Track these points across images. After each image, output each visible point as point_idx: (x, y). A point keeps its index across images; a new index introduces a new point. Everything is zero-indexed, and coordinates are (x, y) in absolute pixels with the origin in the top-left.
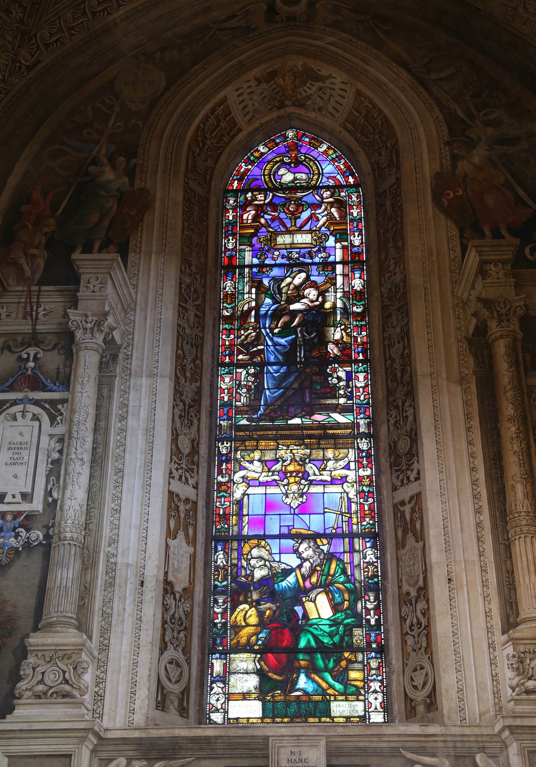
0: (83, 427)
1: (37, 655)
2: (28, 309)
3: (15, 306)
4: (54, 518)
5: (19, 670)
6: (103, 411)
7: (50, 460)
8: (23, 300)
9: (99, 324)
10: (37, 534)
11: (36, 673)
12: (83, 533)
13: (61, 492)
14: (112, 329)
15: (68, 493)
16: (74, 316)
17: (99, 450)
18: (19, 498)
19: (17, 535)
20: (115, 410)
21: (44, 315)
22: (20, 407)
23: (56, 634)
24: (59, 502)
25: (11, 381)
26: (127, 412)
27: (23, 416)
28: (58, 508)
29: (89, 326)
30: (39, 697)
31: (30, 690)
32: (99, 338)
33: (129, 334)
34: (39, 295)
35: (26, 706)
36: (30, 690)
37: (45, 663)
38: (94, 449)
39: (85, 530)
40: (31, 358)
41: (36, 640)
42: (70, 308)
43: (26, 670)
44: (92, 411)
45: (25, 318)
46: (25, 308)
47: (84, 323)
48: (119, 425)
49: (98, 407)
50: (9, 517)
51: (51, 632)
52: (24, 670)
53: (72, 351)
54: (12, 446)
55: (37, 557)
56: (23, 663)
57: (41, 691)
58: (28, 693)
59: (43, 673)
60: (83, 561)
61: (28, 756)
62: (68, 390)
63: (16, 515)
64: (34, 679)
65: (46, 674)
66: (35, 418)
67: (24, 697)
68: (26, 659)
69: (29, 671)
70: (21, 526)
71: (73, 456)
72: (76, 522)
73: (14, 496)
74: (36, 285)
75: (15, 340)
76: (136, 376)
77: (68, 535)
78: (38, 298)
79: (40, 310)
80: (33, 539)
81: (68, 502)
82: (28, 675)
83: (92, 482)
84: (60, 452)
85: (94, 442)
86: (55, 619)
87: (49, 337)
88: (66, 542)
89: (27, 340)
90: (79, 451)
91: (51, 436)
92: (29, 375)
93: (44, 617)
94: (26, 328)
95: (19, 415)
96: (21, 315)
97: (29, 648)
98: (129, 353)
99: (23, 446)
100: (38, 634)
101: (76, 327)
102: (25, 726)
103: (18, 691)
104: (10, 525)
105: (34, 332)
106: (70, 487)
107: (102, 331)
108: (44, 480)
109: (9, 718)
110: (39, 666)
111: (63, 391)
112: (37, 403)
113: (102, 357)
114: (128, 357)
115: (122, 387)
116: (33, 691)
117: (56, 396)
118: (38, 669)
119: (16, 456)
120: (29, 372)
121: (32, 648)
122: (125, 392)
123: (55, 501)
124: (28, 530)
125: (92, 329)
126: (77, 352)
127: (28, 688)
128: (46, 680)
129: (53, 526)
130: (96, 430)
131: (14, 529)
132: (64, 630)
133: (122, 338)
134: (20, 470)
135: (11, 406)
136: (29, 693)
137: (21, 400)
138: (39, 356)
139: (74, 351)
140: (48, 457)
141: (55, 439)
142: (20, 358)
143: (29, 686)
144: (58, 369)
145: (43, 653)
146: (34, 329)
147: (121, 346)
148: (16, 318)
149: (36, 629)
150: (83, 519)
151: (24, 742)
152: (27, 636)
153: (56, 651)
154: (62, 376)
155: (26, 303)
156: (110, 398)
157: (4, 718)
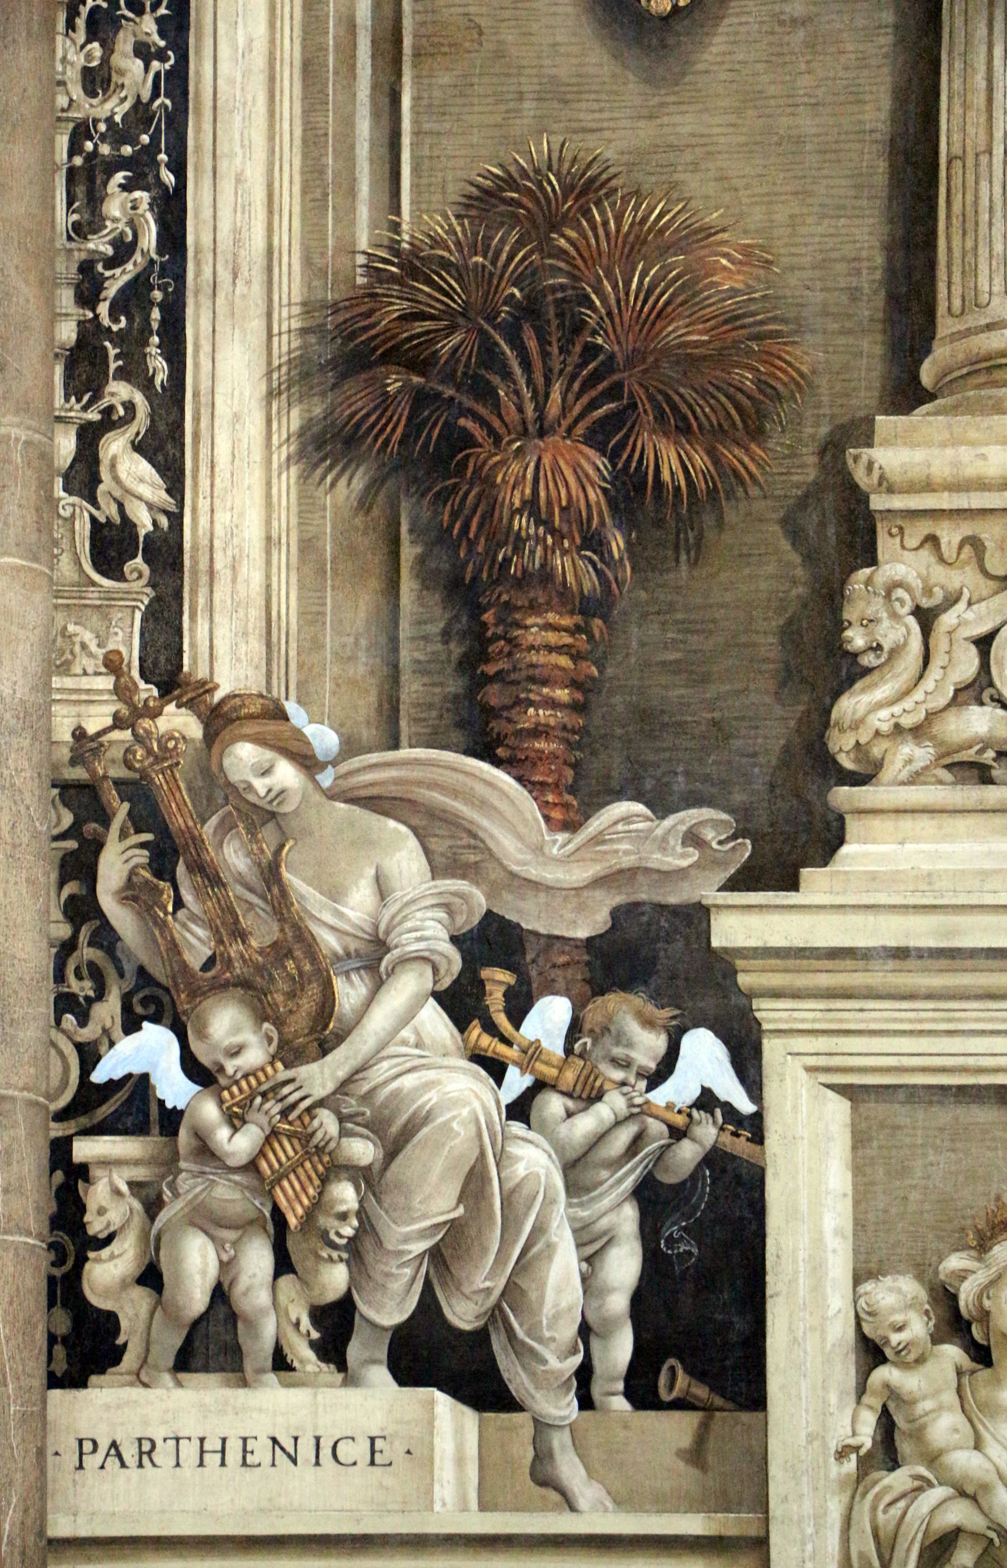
1: (932, 540)
5: (840, 626)
11: (940, 641)
31: (918, 732)
35: (907, 823)
36: (918, 732)
37: (986, 586)
41: (919, 455)
52: (869, 622)
57: (986, 744)
58: (907, 749)
59: (984, 643)
61: (961, 1088)
64: (934, 673)
67: (887, 774)
68: (872, 560)
82: (895, 652)
93: (946, 325)
97: (878, 502)
103: (848, 741)
110: (951, 600)
116: (938, 743)
118: (948, 620)
121: (898, 502)
127: (906, 722)
136: (922, 754)
145: (967, 529)
151: (924, 1014)
157: (792, 884)
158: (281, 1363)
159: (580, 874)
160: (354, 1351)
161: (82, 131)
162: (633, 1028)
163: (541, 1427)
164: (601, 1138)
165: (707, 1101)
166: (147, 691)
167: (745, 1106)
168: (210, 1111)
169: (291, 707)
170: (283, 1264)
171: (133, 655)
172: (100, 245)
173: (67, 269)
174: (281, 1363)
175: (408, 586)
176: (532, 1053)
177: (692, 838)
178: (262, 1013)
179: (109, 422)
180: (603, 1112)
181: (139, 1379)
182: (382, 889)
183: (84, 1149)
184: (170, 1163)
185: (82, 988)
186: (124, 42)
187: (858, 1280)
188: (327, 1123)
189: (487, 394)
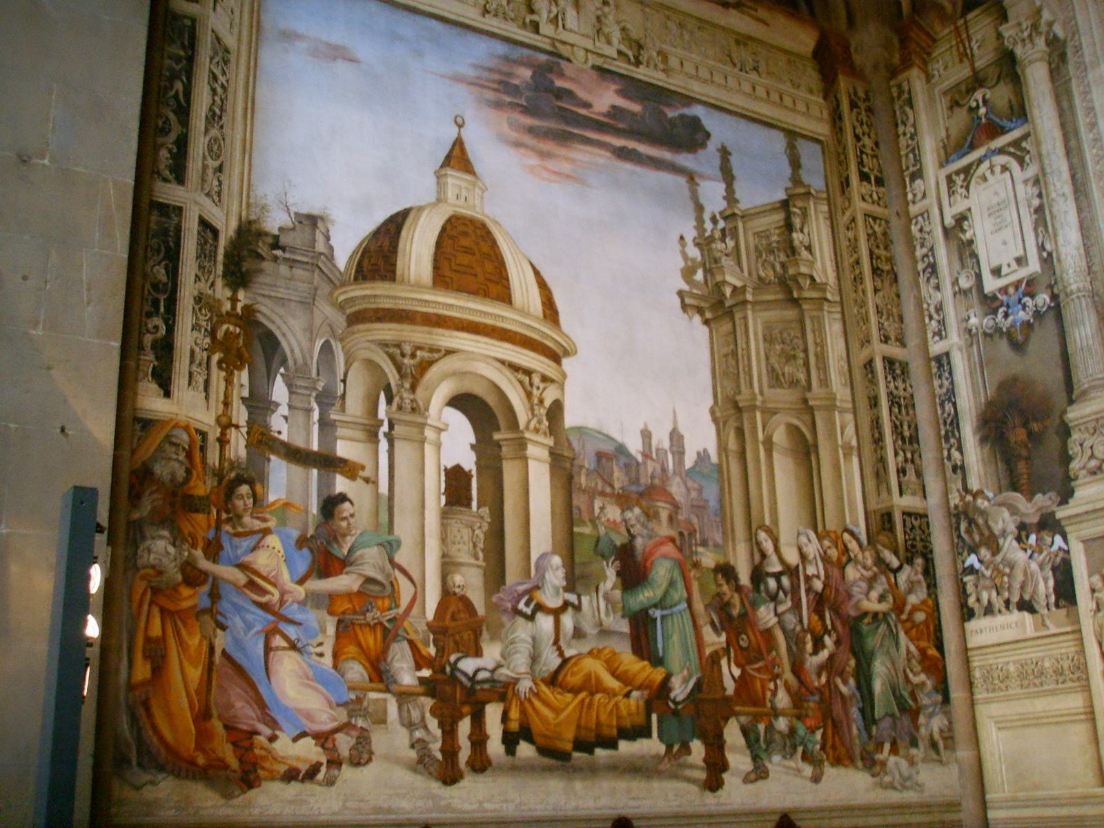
0: (1053, 157)
2: (962, 49)
3: (948, 53)
4: (1054, 274)
6: (1069, 128)
7: (1032, 210)
8: (954, 43)
9: (1035, 27)
10: (1043, 298)
12: (1088, 279)
13: (1053, 242)
14: (1050, 24)
15: (1060, 239)
16: (1008, 31)
17: (1078, 176)
18: (1014, 265)
19: (1024, 307)
20: (1082, 121)
21: (979, 47)
22: (986, 164)
23: (1093, 402)
24: (1054, 255)
25: (969, 139)
26: (1095, 116)
27: (992, 172)
28: (1055, 261)
29: (1026, 34)
30: (1094, 473)
31: (1084, 468)
32: (1040, 42)
33: (1071, 23)
34: (967, 28)
38: (1073, 177)
39: (1089, 274)
40: (981, 104)
42: (1001, 25)
43: (1073, 449)
44: (1058, 134)
45: (961, 61)
46: (958, 49)
47: (1020, 34)
48: (1091, 136)
49: (1063, 125)
50: (1011, 290)
51: (1086, 400)
53: (1017, 74)
54: (992, 211)
55: (1050, 323)
56: (1069, 440)
59: (1091, 447)
60: (1097, 311)
62: (1026, 120)
63: (1017, 285)
65: (1095, 447)
66: (1005, 168)
69: (1077, 449)
70: (1025, 295)
71: (1054, 195)
72: (1078, 269)
73: (1009, 265)
74: (961, 18)
75: (960, 92)
76: (1093, 68)
77: (1074, 287)
78: (967, 32)
79: (973, 43)
80: (1041, 304)
81: (1063, 250)
83: (1082, 216)
84: (1040, 196)
85: (1072, 168)
86: (1086, 386)
87: (991, 69)
88: (1074, 296)
89: (970, 86)
90: (1058, 185)
91: (1026, 182)
92: (985, 125)
93: (1075, 387)
94: (965, 72)
95: (988, 174)
96: (957, 60)
97: (1071, 425)
98: (1077, 44)
99: (1002, 206)
100: (1075, 406)
101: (1014, 45)
102: (1089, 507)
104: (1014, 298)
105: (975, 72)
106: (1060, 232)
107: (1041, 33)
108: (1032, 234)
109: (1071, 502)
110: (1084, 440)
111: (1022, 124)
112: (1001, 151)
113: (1050, 64)
114: (1078, 49)
115: (1081, 88)
117: (1016, 134)
118: (1085, 444)
119: (998, 220)
120: (984, 120)
122: (1086, 93)
123: (1050, 254)
124: (1032, 297)
125: (1030, 36)
126: (1023, 71)
128: (1096, 453)
129: (1056, 283)
130: (1068, 153)
131: (1020, 301)
132: (1099, 394)
133: (1064, 29)
134: (1007, 234)
135: (978, 165)
136: (1084, 472)
137: (985, 156)
138: (988, 96)
139: (1019, 72)
140: (1029, 206)
141: (1030, 184)
142: (971, 110)
143: (1081, 464)
144: (1010, 101)
146: (973, 69)
147: (1065, 42)
148: (953, 66)
149: (1071, 402)
150: (1084, 264)
152: (1065, 412)
153: (1097, 420)
154: (1016, 107)
155: (957, 44)
156: (1072, 106)
157: (1067, 503)
158: (1000, 611)
159: (1034, 510)
160: (1011, 607)
161: (940, 396)
162: (1046, 537)
163: (1042, 616)
164: (1044, 560)
165: (1060, 549)
166: (964, 494)
167: (1066, 548)
168: (983, 568)
169: (985, 491)
170: (998, 594)
171: (961, 488)
172: (946, 415)
173: (941, 421)
174: (1000, 611)
175: (999, 463)
176: (1031, 546)
177: (1050, 499)
178: (989, 548)
179: (951, 446)
180: (1045, 553)
181: (979, 618)
182: (1004, 521)
183: (966, 579)
184: (978, 579)
185: (961, 550)
186: (944, 378)
187: (1090, 576)
188: (1001, 567)
189: (1006, 423)
